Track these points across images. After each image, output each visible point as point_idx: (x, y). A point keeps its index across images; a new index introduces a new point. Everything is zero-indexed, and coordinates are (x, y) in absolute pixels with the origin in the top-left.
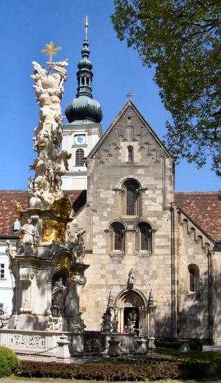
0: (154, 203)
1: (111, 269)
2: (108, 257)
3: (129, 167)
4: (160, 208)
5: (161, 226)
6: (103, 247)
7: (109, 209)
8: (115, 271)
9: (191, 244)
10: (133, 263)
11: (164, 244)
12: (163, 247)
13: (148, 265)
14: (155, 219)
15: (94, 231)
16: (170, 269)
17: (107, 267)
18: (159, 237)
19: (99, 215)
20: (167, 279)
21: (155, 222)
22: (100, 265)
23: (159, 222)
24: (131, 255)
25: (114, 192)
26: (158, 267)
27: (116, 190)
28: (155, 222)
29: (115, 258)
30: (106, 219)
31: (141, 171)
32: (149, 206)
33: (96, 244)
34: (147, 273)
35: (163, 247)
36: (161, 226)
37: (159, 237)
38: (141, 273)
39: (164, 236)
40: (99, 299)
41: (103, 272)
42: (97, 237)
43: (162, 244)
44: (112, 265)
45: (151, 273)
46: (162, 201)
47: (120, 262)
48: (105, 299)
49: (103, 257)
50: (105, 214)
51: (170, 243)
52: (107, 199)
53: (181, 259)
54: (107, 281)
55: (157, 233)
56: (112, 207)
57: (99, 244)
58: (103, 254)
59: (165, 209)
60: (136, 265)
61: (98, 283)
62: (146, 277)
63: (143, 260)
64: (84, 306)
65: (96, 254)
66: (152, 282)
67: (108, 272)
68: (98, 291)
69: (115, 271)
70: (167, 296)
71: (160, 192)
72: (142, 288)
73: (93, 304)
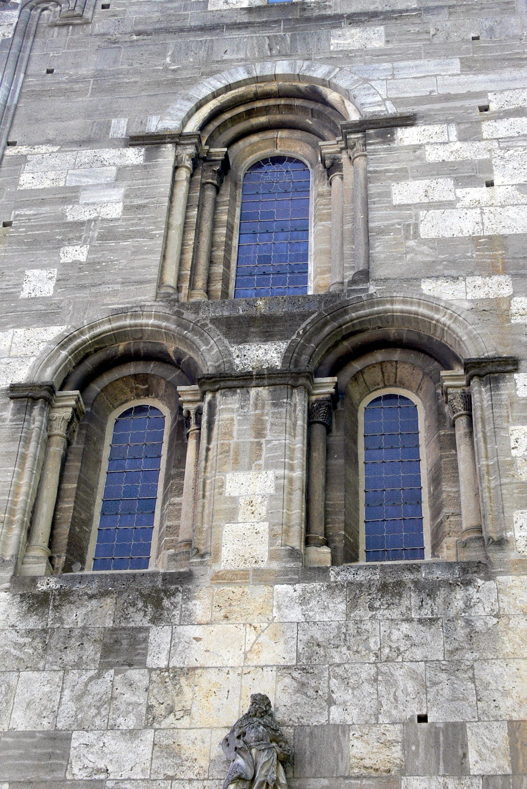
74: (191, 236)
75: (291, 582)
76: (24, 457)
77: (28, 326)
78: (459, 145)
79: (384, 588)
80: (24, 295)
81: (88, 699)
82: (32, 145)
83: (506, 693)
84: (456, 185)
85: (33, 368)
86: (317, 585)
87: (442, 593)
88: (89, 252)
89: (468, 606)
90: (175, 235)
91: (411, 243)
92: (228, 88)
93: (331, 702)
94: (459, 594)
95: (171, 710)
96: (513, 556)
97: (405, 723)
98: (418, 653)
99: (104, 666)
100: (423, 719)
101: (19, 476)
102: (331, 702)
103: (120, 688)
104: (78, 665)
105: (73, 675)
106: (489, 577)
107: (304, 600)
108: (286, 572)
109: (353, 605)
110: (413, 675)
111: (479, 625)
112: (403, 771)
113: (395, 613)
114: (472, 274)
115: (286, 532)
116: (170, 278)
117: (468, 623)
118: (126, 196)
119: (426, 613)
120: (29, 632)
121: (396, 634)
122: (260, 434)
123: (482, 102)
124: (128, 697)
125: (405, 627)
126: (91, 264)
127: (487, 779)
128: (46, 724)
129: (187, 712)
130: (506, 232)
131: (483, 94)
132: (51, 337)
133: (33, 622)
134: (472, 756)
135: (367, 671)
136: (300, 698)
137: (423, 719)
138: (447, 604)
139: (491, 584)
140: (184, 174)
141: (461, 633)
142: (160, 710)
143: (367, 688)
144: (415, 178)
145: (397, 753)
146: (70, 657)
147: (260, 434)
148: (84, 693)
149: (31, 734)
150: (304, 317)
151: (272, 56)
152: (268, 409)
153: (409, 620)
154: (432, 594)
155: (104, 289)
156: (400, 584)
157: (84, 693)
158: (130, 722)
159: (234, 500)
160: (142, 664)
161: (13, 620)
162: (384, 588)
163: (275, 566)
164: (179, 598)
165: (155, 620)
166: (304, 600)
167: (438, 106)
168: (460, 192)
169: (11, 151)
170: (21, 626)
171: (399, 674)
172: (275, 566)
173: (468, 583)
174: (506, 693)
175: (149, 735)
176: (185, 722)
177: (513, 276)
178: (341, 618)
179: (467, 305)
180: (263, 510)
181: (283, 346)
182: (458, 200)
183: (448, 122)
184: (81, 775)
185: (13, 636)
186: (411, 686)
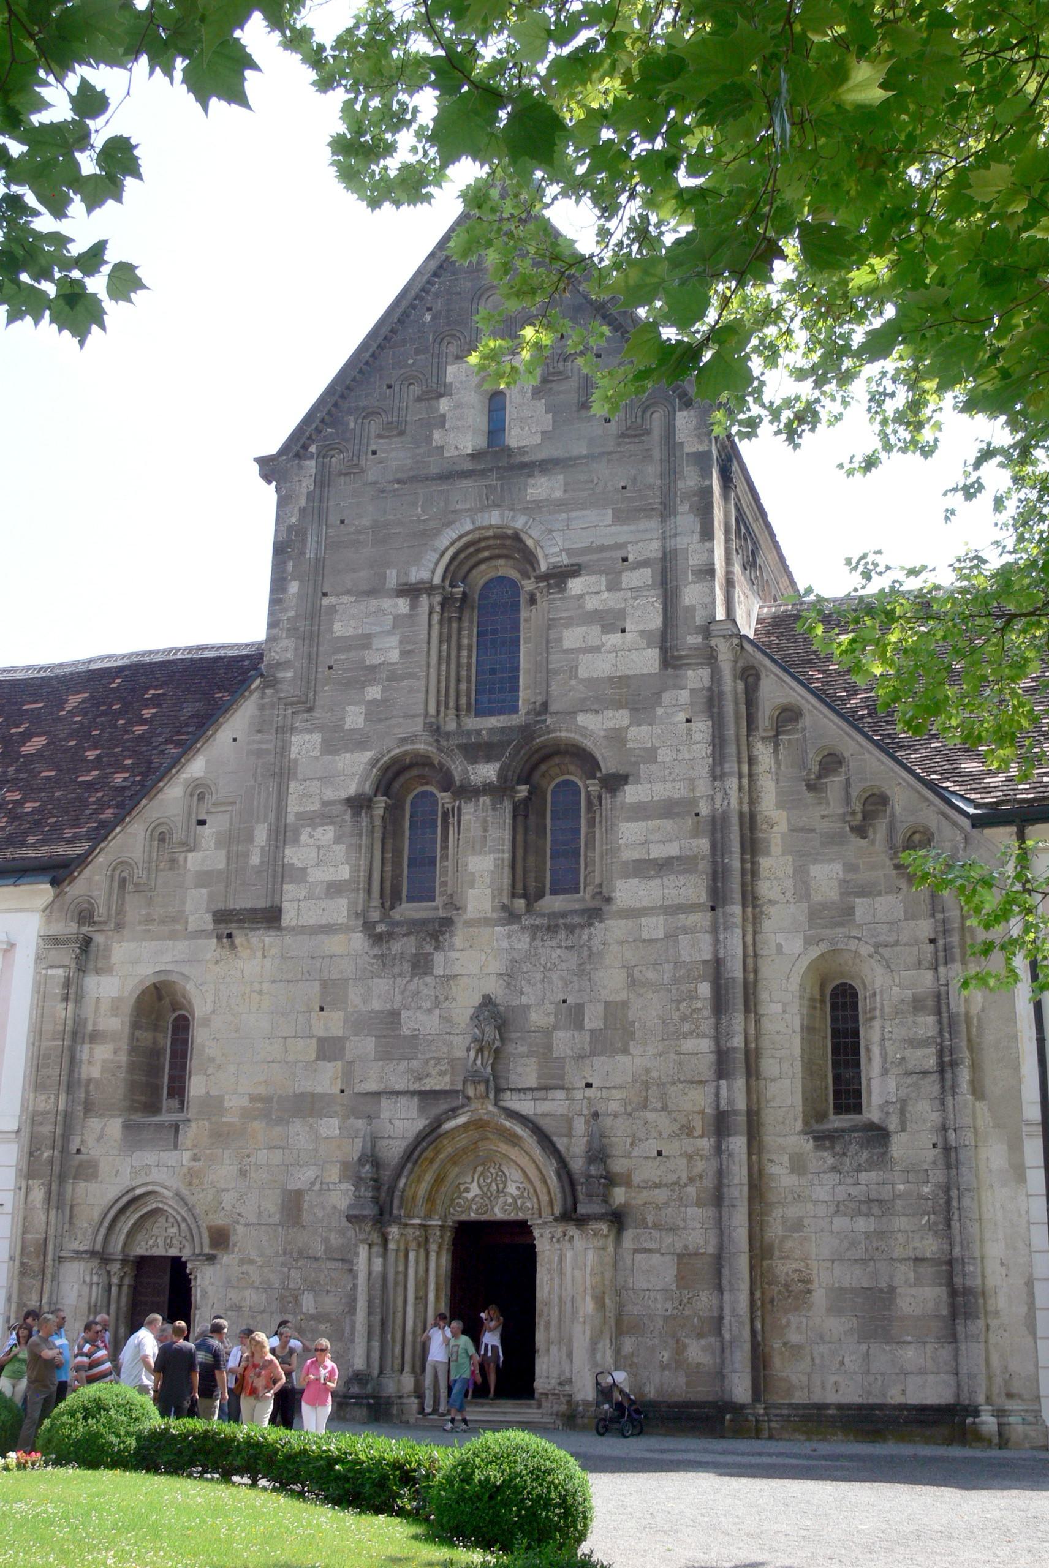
0: (615, 638)
1: (376, 1005)
2: (358, 941)
3: (483, 473)
4: (647, 660)
5: (651, 755)
6: (334, 889)
7: (374, 692)
8: (395, 1015)
9: (833, 839)
10: (496, 966)
11: (673, 850)
12: (662, 867)
13: (581, 972)
14: (620, 718)
15: (294, 807)
16: (705, 989)
17: (354, 996)
18: (641, 812)
19: (320, 728)
20: (689, 1045)
21: (617, 737)
22: (314, 989)
23: (640, 735)
24: (487, 922)
25: (402, 605)
26: (633, 983)
27: (411, 591)
28: (617, 737)
29: (396, 947)
30: (360, 742)
31: (541, 488)
32: (584, 658)
33: (300, 875)
34: (574, 1016)
35: (662, 867)
36: (651, 755)
37: (641, 812)
38: (538, 1018)
39: (669, 809)
40: (303, 1177)
41: (333, 1024)
42: (304, 838)
43: (657, 852)
44: (381, 985)
45: (593, 1019)
46: (655, 622)
47: (421, 965)
48: (334, 1173)
49: (335, 944)
50: (354, 718)
51: (703, 844)
52: (364, 642)
53: (767, 925)
54: (348, 1074)
55: (631, 794)
56: (392, 677)
57: (320, 875)
58: (328, 929)
59: (670, 660)
60: (509, 976)
61: (306, 1085)
62: (564, 1041)
63: (551, 951)
64: (219, 1220)
65: (301, 931)
66: (599, 1069)
67: (359, 1025)
68: (299, 1132)
69: (395, 1015)
70: (687, 1145)
71: (645, 576)
72: (544, 1107)
73: (272, 1205)
74: (444, 667)
75: (503, 925)
76: (360, 846)
77: (352, 752)
78: (606, 595)
79: (549, 928)
80: (347, 727)
81: (407, 993)
82: (337, 595)
83: (604, 987)
84: (603, 632)
85: (358, 784)
86: (515, 927)
87: (578, 931)
88: (383, 691)
89: (590, 939)
90: (433, 672)
91: (573, 682)
92: (461, 537)
93: (522, 993)
94: (586, 932)
95: (446, 999)
96: (614, 908)
97: (557, 1004)
98: (564, 966)
99: (413, 975)
100: (565, 1001)
101: (359, 859)
102: (522, 993)
103: (422, 987)
104: (400, 975)
105: (399, 980)
106: (601, 921)
107: (509, 936)
108: (500, 919)
109: (533, 939)
110: (561, 978)
111: (594, 949)
112: (555, 1028)
113: (554, 943)
114: (607, 708)
115: (500, 894)
116: (432, 711)
117: (589, 948)
118: (401, 642)
119: (569, 943)
120: (375, 956)
121: (554, 955)
122: (485, 830)
123: (621, 553)
124: (425, 991)
125: (558, 951)
126: (384, 701)
127: (592, 1031)
128: (388, 1007)
129: (454, 999)
130: (630, 673)
131: (623, 546)
132: (366, 760)
133: (376, 951)
134: (586, 1020)
135: (539, 976)
136: (507, 991)
137: (565, 1001)
138: (580, 937)
139: (602, 925)
140: (436, 617)
141: (586, 953)
142: (442, 998)
143: (539, 985)
144: (578, 625)
145: (552, 1019)
146: (396, 970)
147: (485, 830)
148: (405, 990)
149: (382, 1012)
150: (509, 743)
151: (488, 506)
152: (490, 812)
153: (560, 947)
154: (572, 932)
155: (393, 722)
156: (557, 926)
157: (405, 990)
158: (427, 1005)
159: (473, 874)
160: (432, 974)
161: (366, 949)
162: (549, 928)
163: (495, 915)
164: (447, 936)
165: (437, 948)
166: (509, 936)
167: (595, 557)
168: (605, 638)
169: (325, 601)
170: (371, 953)
171: (554, 977)
172: (495, 915)
173: (591, 925)
174: (604, 987)
175: (437, 1012)
176: (454, 1005)
177: (631, 709)
178: (527, 946)
179: (602, 733)
180: (488, 880)
181: (497, 765)
182: (603, 645)
183: (601, 572)
184: (408, 1032)
185: (367, 958)
186: (560, 984)
